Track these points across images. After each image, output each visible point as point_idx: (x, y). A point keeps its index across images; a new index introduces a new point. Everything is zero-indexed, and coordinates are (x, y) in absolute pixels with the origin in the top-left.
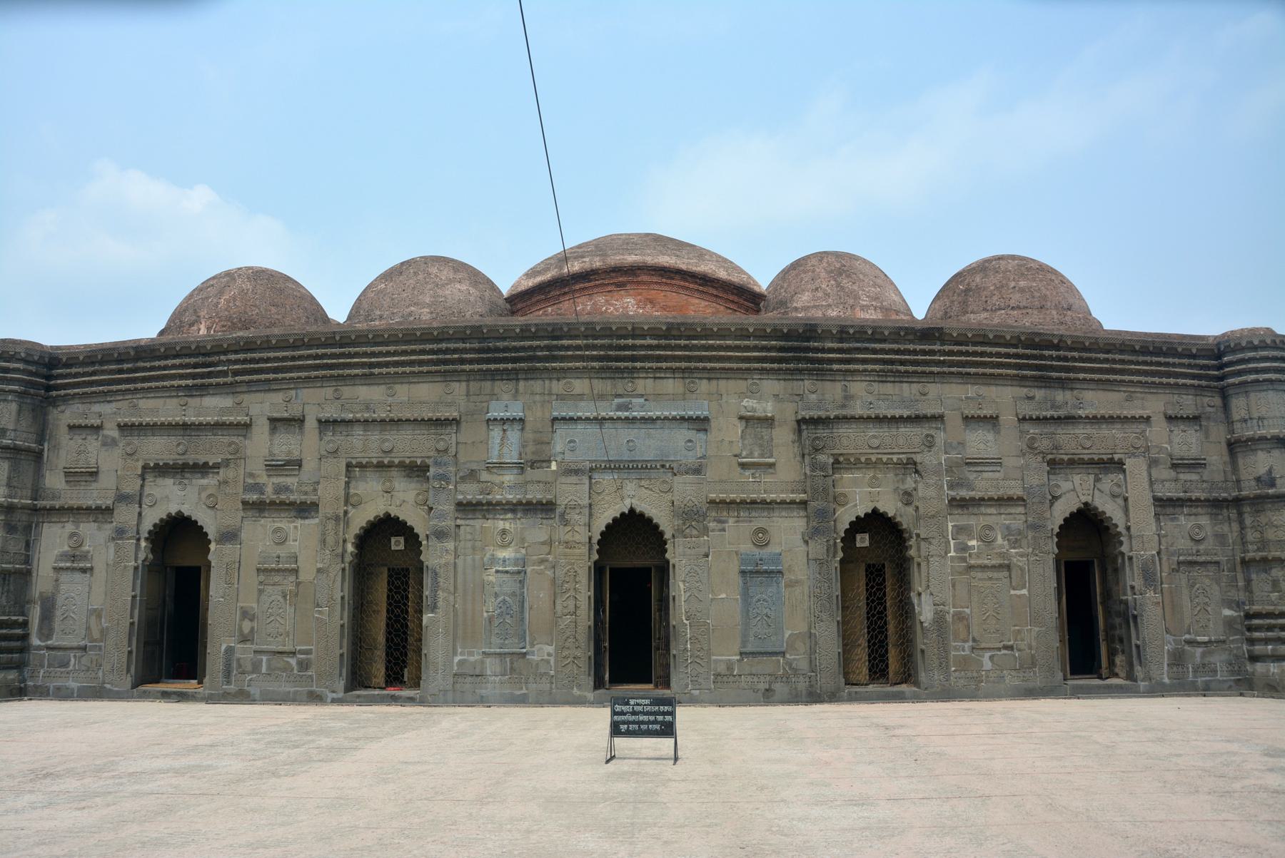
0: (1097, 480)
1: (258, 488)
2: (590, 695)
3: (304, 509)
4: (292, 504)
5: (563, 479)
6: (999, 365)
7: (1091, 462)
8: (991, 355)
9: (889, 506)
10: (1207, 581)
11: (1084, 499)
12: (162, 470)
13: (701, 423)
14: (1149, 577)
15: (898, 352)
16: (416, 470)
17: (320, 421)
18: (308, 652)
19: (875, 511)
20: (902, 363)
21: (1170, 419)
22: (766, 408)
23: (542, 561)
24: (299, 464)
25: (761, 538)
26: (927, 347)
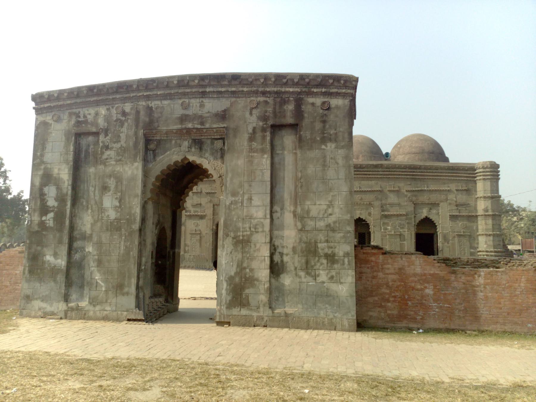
0: (431, 209)
3: (202, 217)
4: (198, 215)
6: (399, 175)
7: (428, 204)
8: (397, 172)
10: (465, 241)
11: (425, 215)
14: (446, 238)
15: (368, 171)
19: (359, 218)
20: (369, 175)
21: (457, 190)
26: (377, 170)
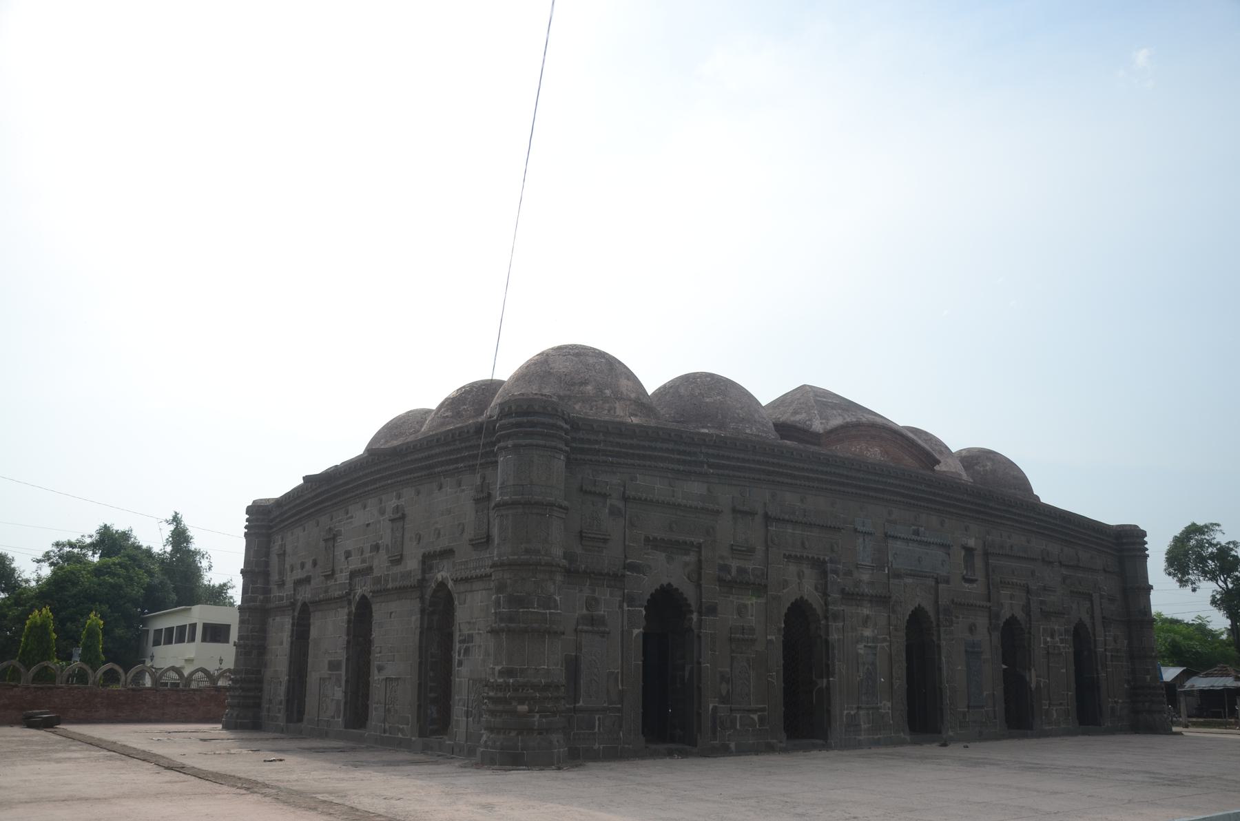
1: (725, 568)
2: (908, 738)
3: (760, 589)
5: (892, 581)
9: (1020, 615)
12: (654, 543)
13: (946, 547)
16: (820, 566)
17: (767, 517)
18: (763, 710)
22: (971, 543)
23: (884, 640)
24: (751, 550)
25: (972, 629)
